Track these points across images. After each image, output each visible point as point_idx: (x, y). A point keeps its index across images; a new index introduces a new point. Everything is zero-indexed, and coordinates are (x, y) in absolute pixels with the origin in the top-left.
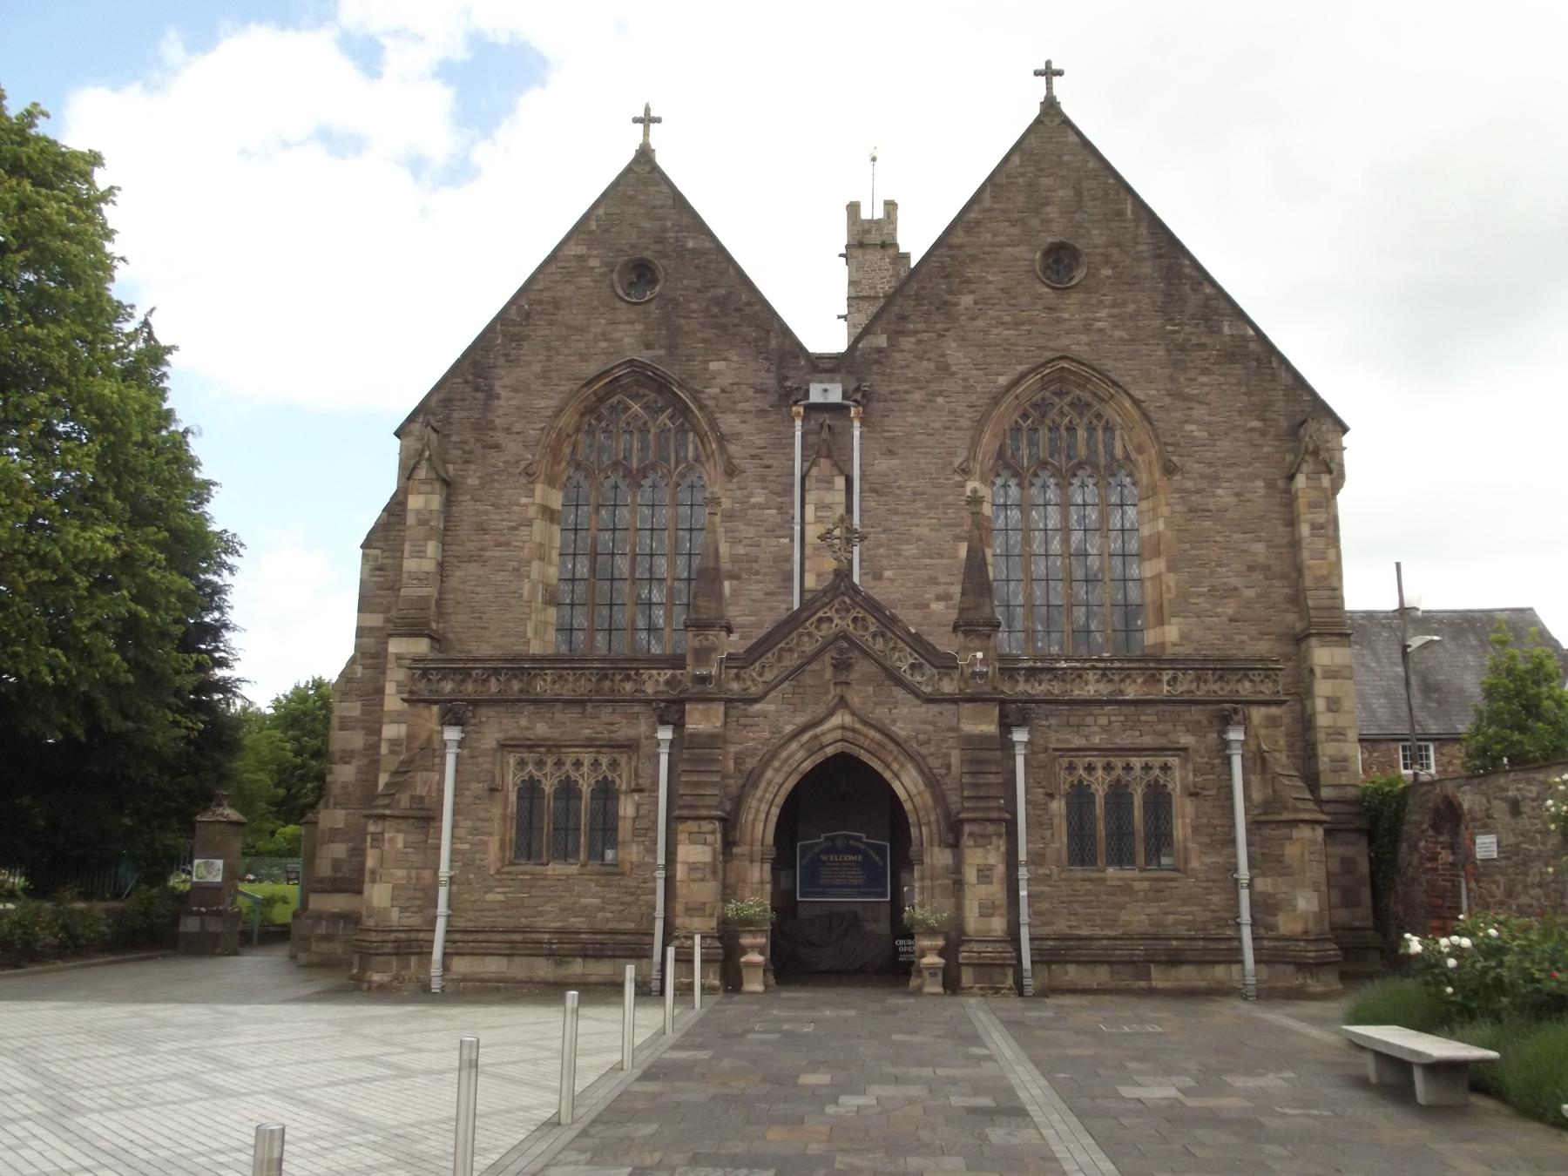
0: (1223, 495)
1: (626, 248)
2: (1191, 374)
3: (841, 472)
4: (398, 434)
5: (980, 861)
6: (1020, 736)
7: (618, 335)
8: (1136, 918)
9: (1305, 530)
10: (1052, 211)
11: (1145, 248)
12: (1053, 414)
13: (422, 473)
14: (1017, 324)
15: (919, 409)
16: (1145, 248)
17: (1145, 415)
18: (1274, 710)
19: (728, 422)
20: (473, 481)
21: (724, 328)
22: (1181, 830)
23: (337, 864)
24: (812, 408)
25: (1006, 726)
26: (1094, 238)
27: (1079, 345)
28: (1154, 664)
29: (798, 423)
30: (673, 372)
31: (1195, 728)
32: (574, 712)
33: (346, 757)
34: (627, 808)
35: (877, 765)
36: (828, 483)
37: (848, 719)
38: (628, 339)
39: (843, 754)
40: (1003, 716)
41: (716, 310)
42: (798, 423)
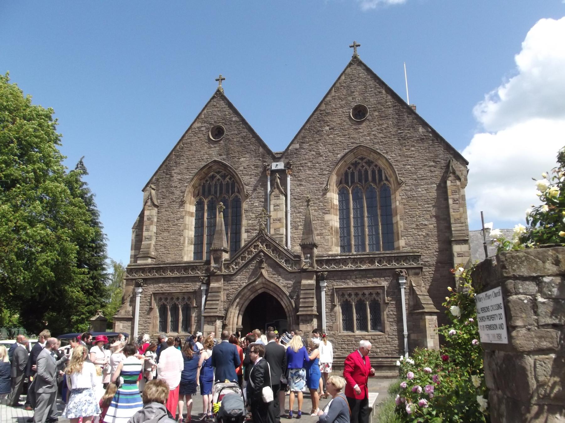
1: (213, 123)
2: (408, 147)
3: (282, 193)
4: (143, 191)
5: (305, 330)
7: (211, 152)
9: (451, 201)
11: (390, 103)
12: (359, 167)
15: (310, 169)
16: (390, 103)
17: (390, 165)
20: (166, 205)
21: (244, 147)
26: (371, 102)
27: (366, 141)
29: (269, 177)
35: (275, 296)
36: (277, 197)
38: (213, 153)
40: (317, 277)
41: (242, 140)
42: (269, 177)
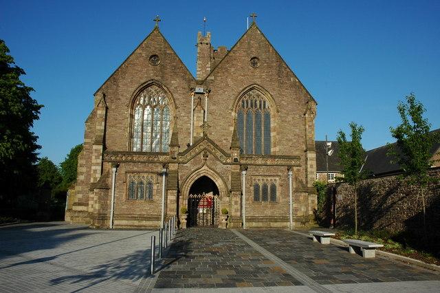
0: (290, 118)
6: (244, 172)
8: (268, 212)
10: (253, 49)
13: (100, 105)
14: (244, 76)
18: (299, 168)
19: (176, 96)
22: (278, 194)
23: (79, 199)
25: (241, 170)
28: (274, 157)
30: (164, 82)
31: (282, 171)
32: (143, 165)
34: (155, 187)
37: (206, 168)
39: (205, 176)
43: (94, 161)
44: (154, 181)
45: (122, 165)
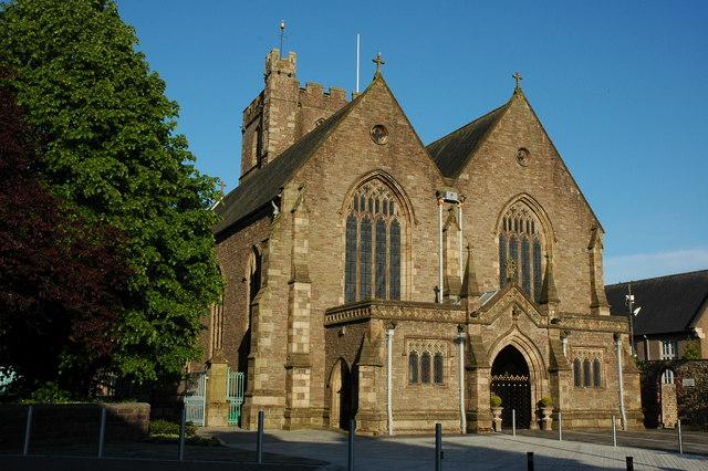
8: (594, 404)
13: (300, 208)
19: (415, 202)
22: (603, 375)
24: (446, 201)
30: (396, 177)
33: (267, 334)
43: (296, 312)
44: (444, 353)
45: (400, 324)
